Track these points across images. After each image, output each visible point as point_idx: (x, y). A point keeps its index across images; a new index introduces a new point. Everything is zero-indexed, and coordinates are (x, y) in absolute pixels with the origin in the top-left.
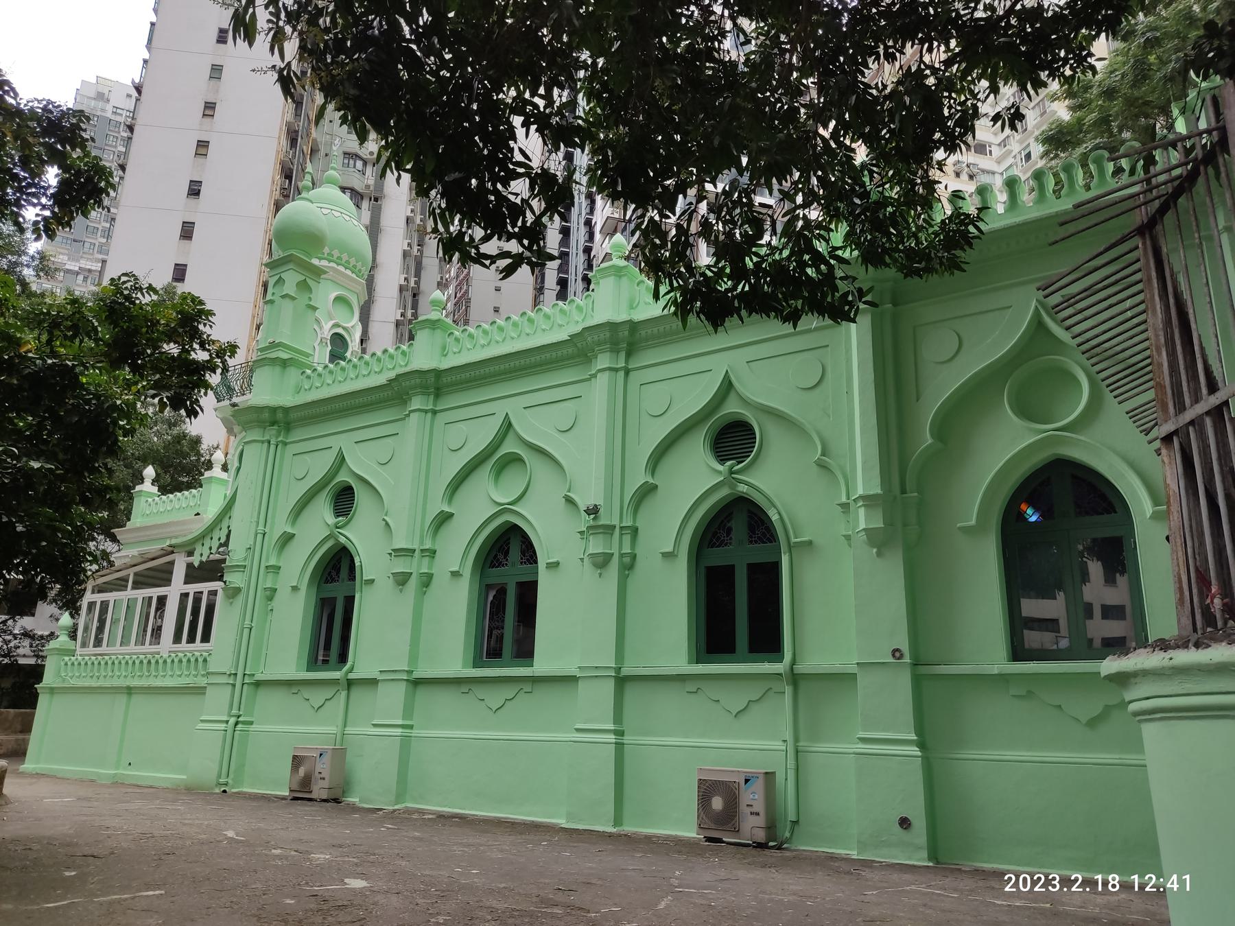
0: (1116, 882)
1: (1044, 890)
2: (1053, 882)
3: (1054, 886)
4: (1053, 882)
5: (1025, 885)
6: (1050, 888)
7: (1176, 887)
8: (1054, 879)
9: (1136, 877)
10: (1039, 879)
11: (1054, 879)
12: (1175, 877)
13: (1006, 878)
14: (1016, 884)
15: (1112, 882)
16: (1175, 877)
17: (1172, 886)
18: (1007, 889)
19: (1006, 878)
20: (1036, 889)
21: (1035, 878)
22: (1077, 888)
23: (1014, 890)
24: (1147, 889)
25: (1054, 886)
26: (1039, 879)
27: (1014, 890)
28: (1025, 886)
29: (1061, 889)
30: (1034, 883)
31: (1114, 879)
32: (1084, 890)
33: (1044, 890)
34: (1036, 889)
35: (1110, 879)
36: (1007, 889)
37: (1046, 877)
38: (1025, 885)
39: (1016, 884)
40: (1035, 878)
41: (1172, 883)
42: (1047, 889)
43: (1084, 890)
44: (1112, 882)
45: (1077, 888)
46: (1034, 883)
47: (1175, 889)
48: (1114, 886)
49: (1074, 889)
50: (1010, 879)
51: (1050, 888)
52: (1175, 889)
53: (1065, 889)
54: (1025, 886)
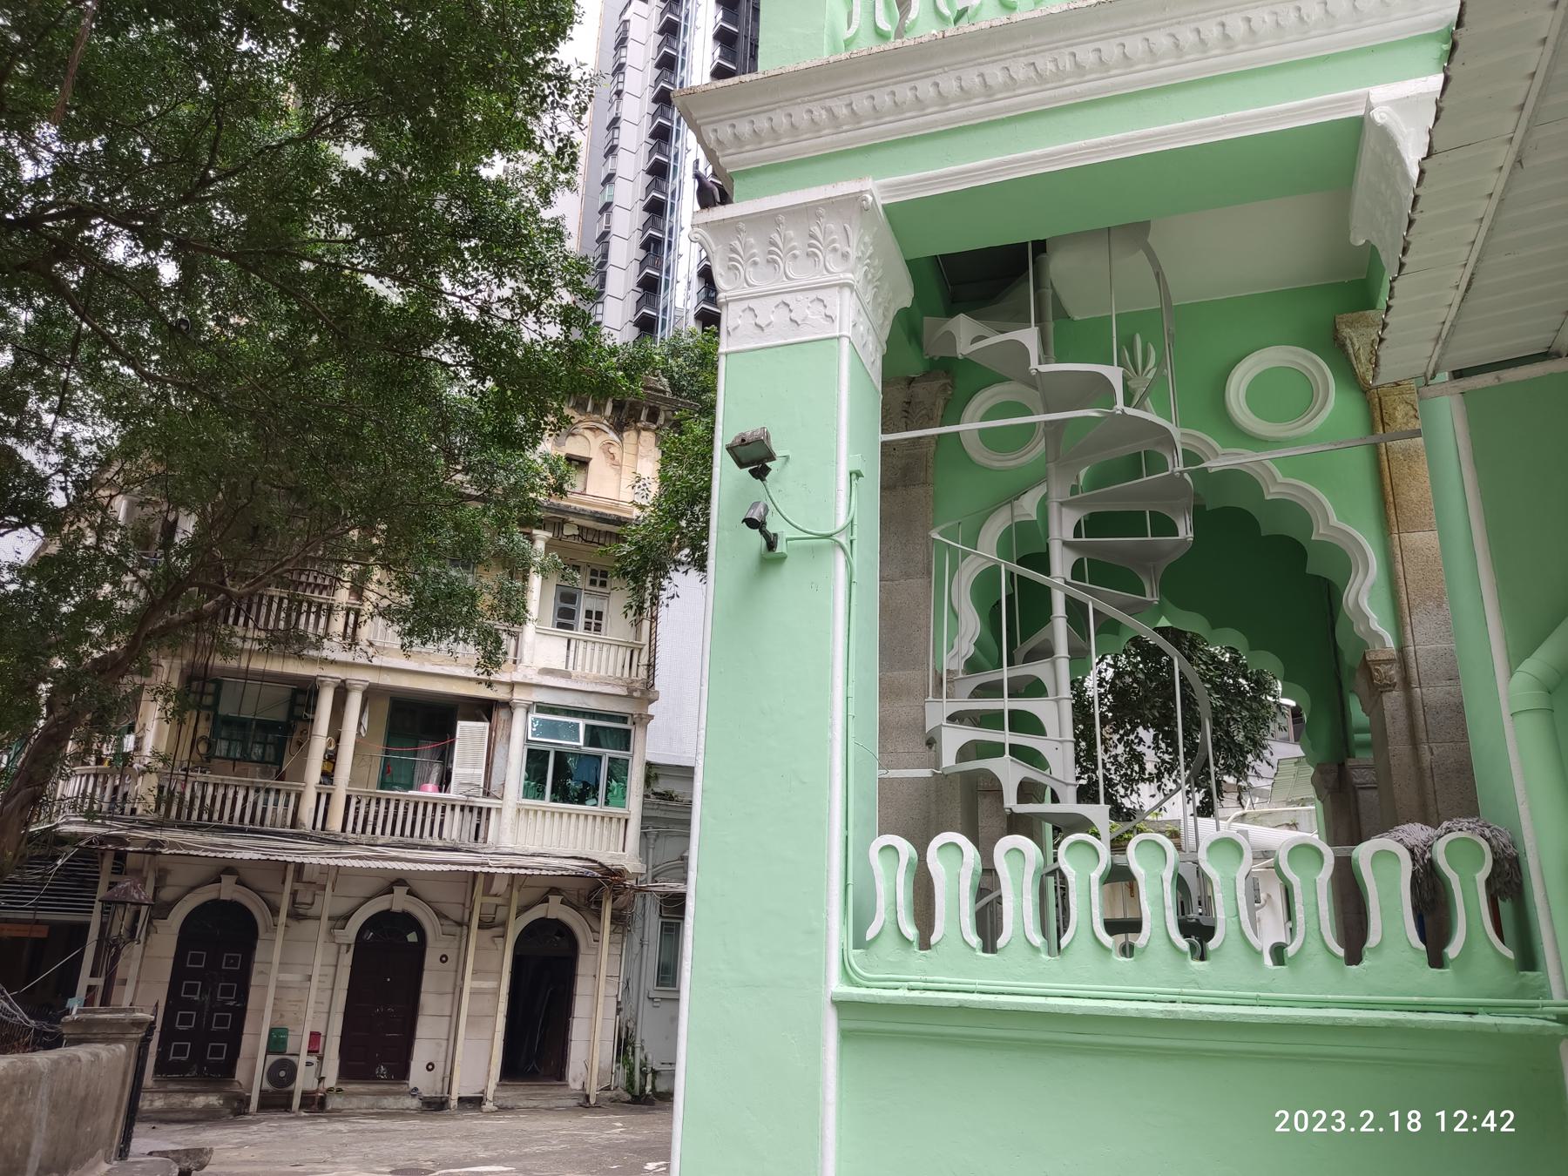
0: (1412, 1121)
1: (1325, 1130)
2: (1337, 1121)
3: (1339, 1126)
4: (1337, 1121)
5: (1301, 1125)
6: (1333, 1128)
8: (1338, 1116)
9: (1442, 1114)
10: (1320, 1116)
11: (1338, 1116)
12: (1491, 1113)
13: (1277, 1115)
14: (1290, 1124)
16: (1491, 1113)
17: (1488, 1125)
18: (1278, 1129)
19: (1277, 1115)
20: (1316, 1129)
21: (1314, 1115)
22: (1368, 1127)
23: (1288, 1130)
25: (1339, 1126)
26: (1320, 1116)
27: (1288, 1130)
28: (1301, 1125)
29: (1347, 1128)
30: (1313, 1122)
32: (1377, 1130)
33: (1325, 1130)
34: (1316, 1129)
36: (1278, 1129)
37: (1328, 1115)
38: (1301, 1125)
39: (1290, 1124)
40: (1314, 1115)
41: (1489, 1122)
42: (1329, 1129)
43: (1377, 1130)
44: (1416, 1121)
45: (1368, 1127)
46: (1313, 1122)
47: (1492, 1130)
48: (1414, 1125)
49: (1363, 1129)
50: (1282, 1116)
51: (1333, 1128)
52: (1492, 1130)
53: (1352, 1130)
54: (1301, 1125)
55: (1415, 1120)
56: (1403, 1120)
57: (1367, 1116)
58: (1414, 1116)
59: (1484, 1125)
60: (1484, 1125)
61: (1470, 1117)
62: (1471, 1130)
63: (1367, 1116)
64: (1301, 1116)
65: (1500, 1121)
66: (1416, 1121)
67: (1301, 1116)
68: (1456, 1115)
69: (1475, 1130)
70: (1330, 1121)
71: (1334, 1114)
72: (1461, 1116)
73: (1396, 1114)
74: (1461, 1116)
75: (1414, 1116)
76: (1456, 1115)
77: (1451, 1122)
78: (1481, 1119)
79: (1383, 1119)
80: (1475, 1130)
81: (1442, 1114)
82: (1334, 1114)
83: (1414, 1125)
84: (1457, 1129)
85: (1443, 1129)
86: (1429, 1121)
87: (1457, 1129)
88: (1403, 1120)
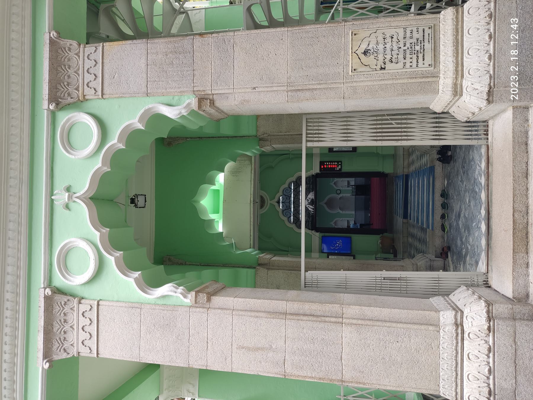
6: (517, 80)
7: (516, 26)
8: (513, 78)
9: (512, 43)
12: (512, 26)
15: (514, 53)
16: (512, 26)
17: (516, 27)
23: (517, 95)
24: (517, 38)
27: (517, 95)
31: (513, 52)
35: (513, 54)
40: (512, 86)
41: (515, 27)
45: (516, 68)
57: (512, 68)
58: (513, 52)
61: (513, 33)
62: (517, 33)
65: (514, 23)
72: (513, 36)
74: (513, 36)
78: (514, 30)
82: (512, 80)
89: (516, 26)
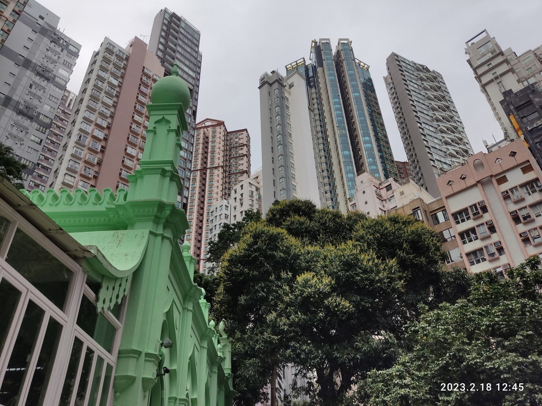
3: (463, 389)
6: (461, 389)
7: (516, 389)
8: (463, 385)
10: (456, 385)
12: (516, 384)
14: (446, 388)
15: (488, 387)
16: (516, 384)
18: (442, 390)
21: (454, 385)
26: (456, 385)
28: (450, 389)
30: (454, 387)
32: (476, 390)
36: (442, 390)
39: (446, 388)
40: (454, 385)
41: (515, 387)
43: (476, 390)
44: (490, 387)
48: (489, 389)
49: (471, 390)
51: (461, 389)
55: (489, 387)
56: (485, 387)
57: (473, 385)
58: (489, 385)
59: (513, 388)
60: (513, 388)
61: (508, 385)
62: (508, 390)
63: (473, 385)
64: (450, 385)
66: (490, 387)
67: (450, 385)
68: (503, 385)
69: (510, 390)
70: (460, 387)
71: (461, 385)
72: (505, 385)
73: (482, 384)
74: (505, 385)
75: (489, 385)
76: (503, 385)
77: (502, 387)
79: (478, 387)
80: (510, 390)
81: (498, 384)
82: (461, 385)
83: (489, 389)
84: (504, 390)
85: (499, 390)
86: (494, 387)
87: (504, 390)
88: (485, 387)
89: (516, 389)
